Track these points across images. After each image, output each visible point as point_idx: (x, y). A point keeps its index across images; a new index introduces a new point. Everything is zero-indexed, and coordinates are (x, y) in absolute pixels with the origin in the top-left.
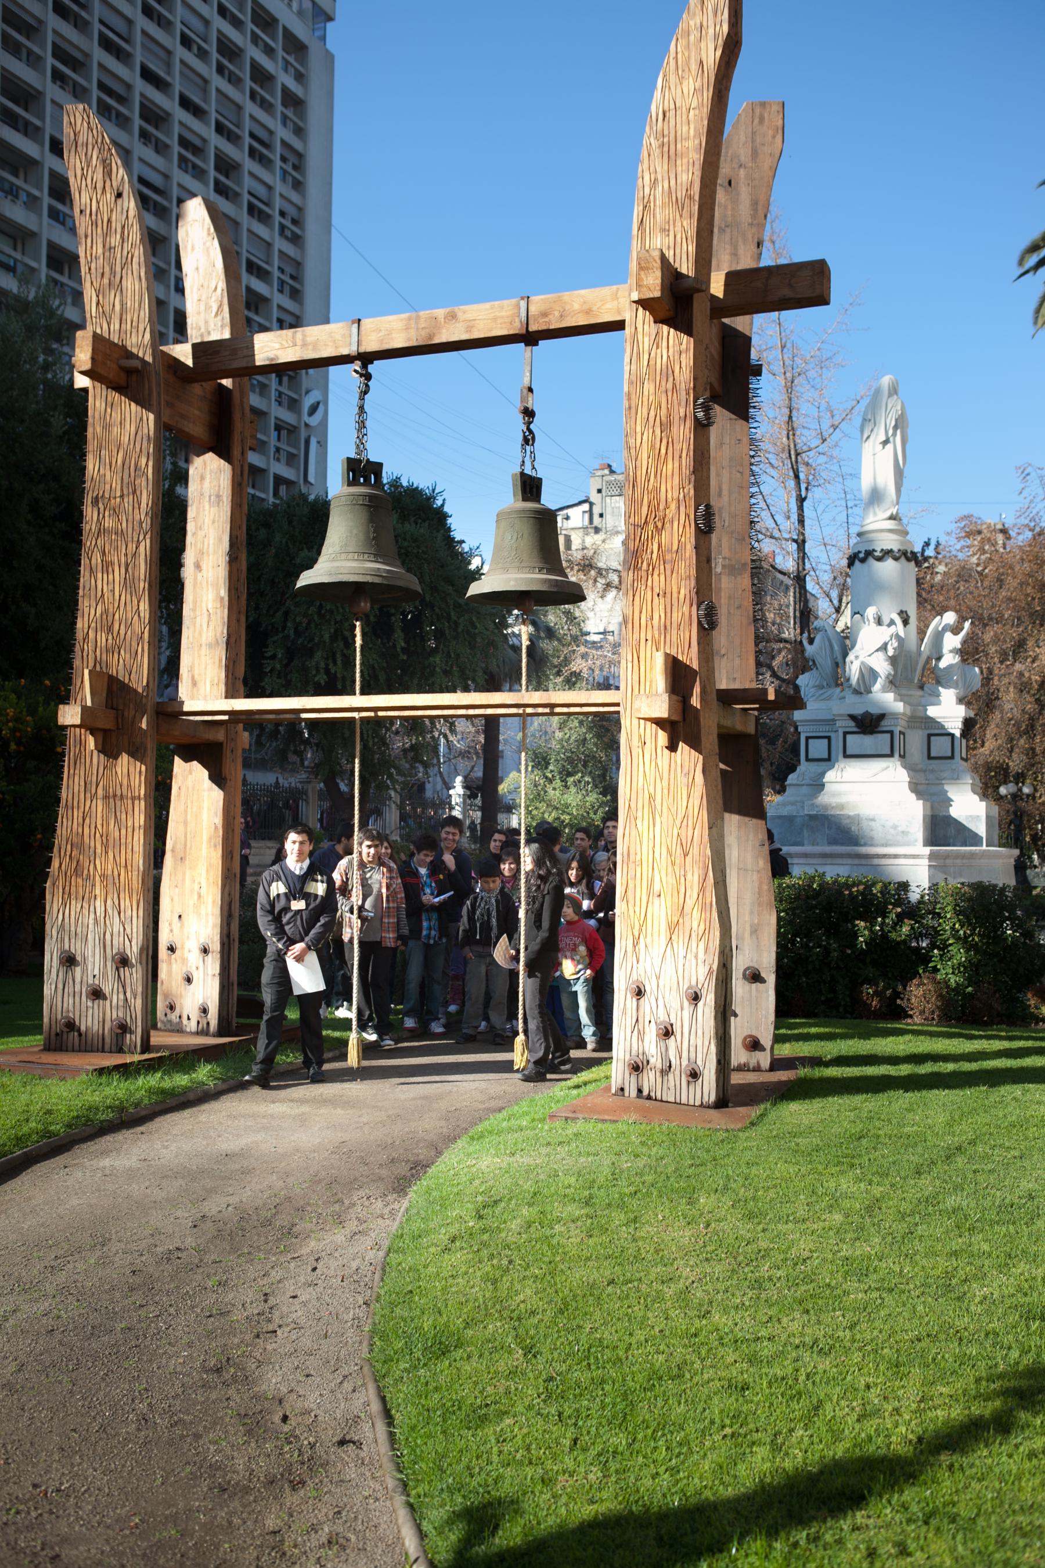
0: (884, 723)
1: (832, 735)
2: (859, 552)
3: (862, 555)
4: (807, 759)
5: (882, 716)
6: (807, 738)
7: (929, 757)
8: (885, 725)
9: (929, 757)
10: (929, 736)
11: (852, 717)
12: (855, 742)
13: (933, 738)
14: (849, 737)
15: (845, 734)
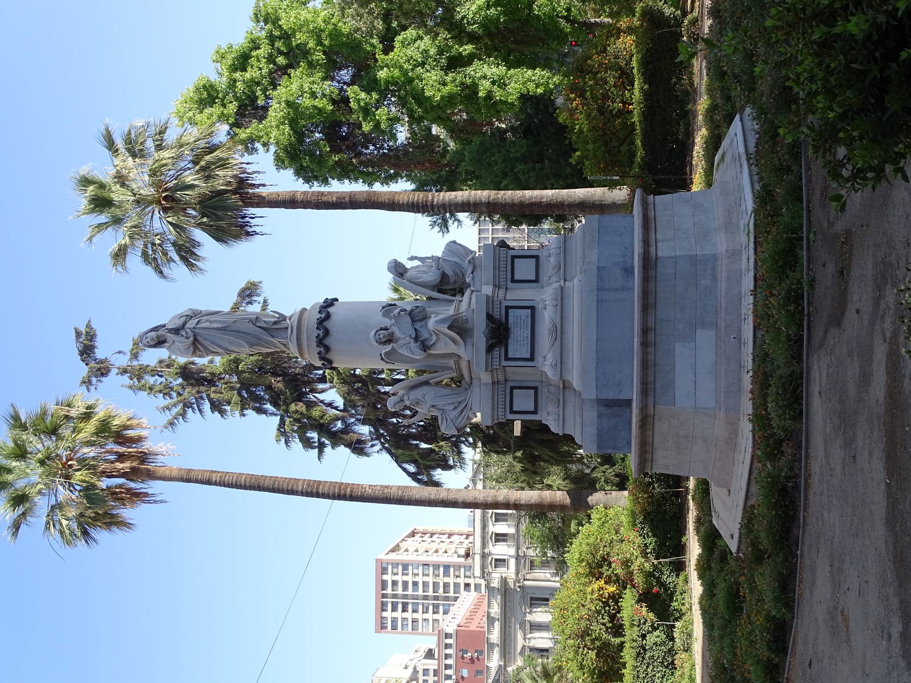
0: (496, 315)
1: (510, 384)
2: (319, 353)
3: (322, 349)
4: (535, 412)
5: (489, 317)
6: (512, 412)
7: (536, 281)
8: (498, 314)
9: (536, 281)
10: (513, 281)
11: (490, 349)
12: (518, 346)
13: (516, 278)
14: (510, 355)
15: (507, 359)
